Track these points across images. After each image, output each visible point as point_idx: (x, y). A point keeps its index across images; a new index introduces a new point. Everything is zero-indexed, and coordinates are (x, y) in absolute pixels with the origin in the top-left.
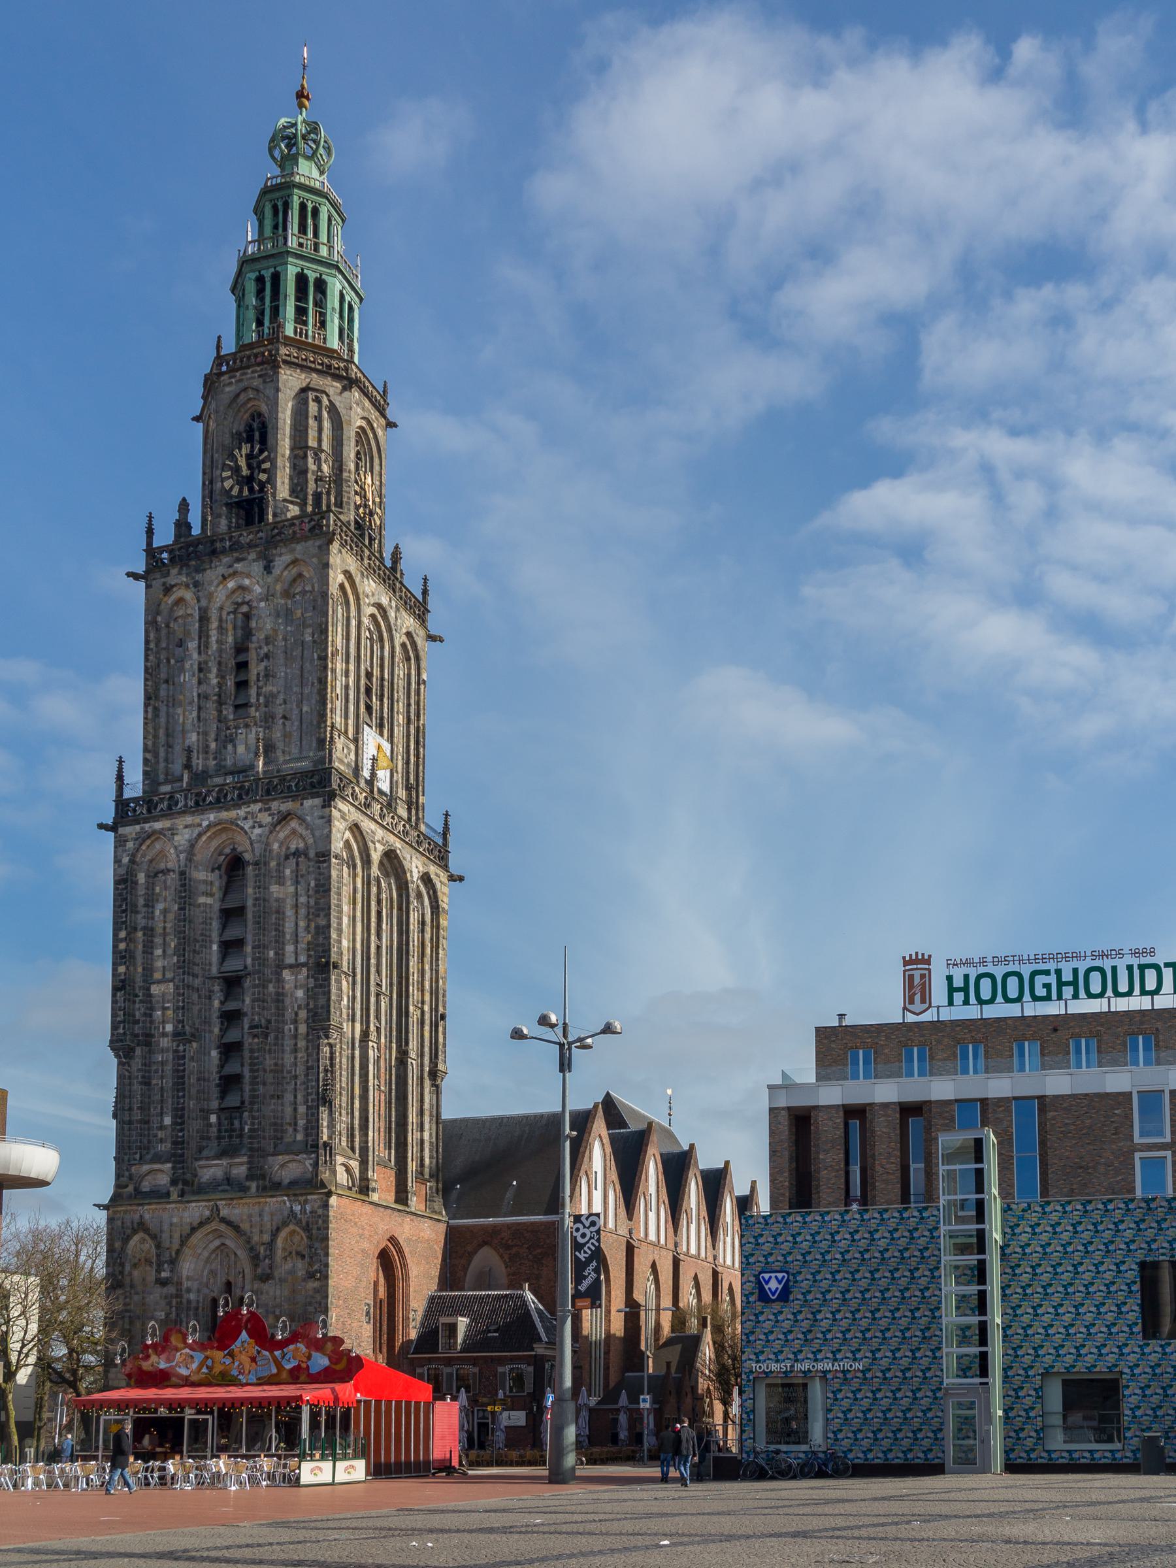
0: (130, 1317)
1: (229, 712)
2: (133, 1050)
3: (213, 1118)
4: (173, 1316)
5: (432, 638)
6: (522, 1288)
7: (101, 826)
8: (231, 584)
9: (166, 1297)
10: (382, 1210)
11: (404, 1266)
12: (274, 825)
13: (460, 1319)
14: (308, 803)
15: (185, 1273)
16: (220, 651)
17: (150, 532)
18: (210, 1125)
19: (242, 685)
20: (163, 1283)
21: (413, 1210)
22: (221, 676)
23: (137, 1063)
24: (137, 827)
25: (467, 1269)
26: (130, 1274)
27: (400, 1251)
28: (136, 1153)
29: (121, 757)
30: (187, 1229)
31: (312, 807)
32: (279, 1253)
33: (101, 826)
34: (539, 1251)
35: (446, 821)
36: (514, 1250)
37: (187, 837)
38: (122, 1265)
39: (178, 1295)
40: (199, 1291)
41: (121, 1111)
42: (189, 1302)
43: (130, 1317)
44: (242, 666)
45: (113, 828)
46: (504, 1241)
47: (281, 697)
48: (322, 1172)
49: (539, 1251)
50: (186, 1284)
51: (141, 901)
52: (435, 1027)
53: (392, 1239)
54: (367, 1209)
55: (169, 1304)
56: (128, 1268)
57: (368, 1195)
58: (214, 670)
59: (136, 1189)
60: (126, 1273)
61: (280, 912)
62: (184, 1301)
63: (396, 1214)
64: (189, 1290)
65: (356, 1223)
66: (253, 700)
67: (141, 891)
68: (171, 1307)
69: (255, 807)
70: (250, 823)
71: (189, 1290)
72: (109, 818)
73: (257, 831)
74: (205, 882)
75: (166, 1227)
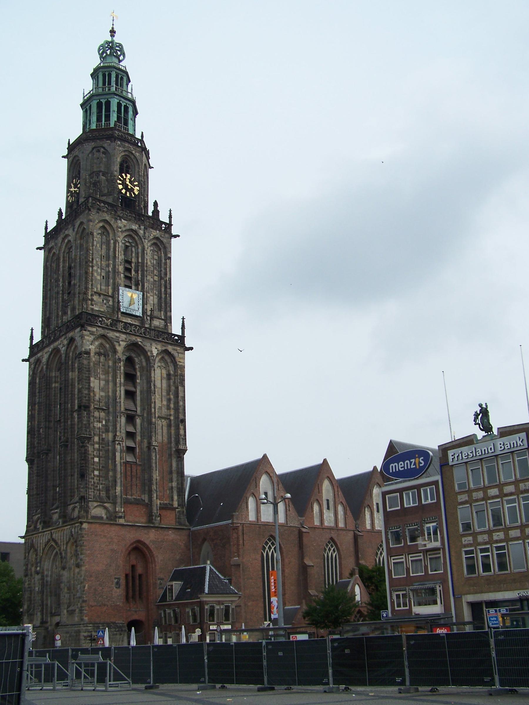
0: (30, 591)
1: (66, 297)
2: (33, 460)
8: (66, 241)
10: (129, 527)
11: (152, 556)
12: (68, 344)
13: (174, 582)
15: (45, 567)
16: (63, 271)
18: (56, 493)
19: (70, 283)
20: (37, 573)
21: (157, 525)
22: (64, 282)
23: (35, 468)
25: (200, 554)
26: (31, 569)
27: (148, 547)
29: (32, 328)
32: (69, 555)
33: (23, 360)
40: (51, 576)
41: (29, 492)
42: (47, 582)
43: (30, 591)
47: (78, 284)
50: (46, 573)
51: (37, 391)
52: (177, 429)
53: (139, 541)
54: (114, 528)
57: (116, 521)
58: (61, 280)
61: (73, 385)
62: (45, 582)
63: (141, 528)
64: (47, 576)
65: (105, 536)
70: (61, 346)
71: (47, 576)
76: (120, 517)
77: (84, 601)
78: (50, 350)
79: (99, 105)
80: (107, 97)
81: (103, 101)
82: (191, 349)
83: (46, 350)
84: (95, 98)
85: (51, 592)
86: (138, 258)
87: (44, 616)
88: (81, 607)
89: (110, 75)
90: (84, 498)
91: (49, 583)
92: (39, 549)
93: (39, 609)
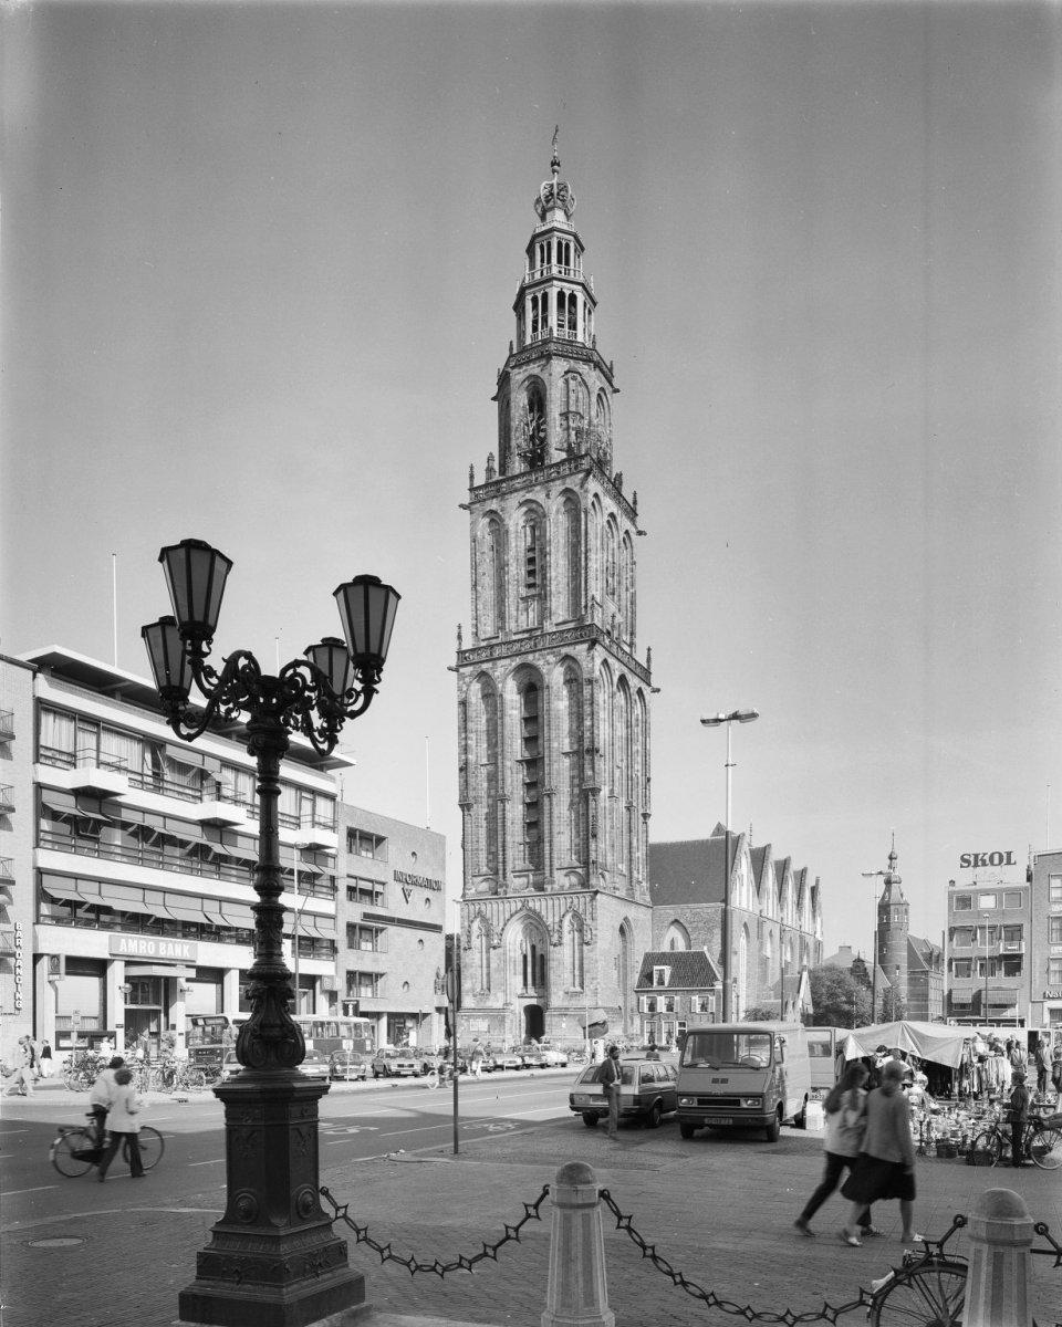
5: (640, 533)
7: (450, 669)
17: (472, 477)
30: (507, 916)
35: (649, 655)
39: (505, 954)
45: (457, 670)
53: (626, 919)
55: (499, 959)
72: (453, 662)
76: (618, 889)
77: (598, 983)
79: (561, 295)
80: (575, 287)
81: (567, 293)
82: (658, 690)
84: (555, 282)
86: (613, 555)
89: (567, 246)
92: (495, 918)
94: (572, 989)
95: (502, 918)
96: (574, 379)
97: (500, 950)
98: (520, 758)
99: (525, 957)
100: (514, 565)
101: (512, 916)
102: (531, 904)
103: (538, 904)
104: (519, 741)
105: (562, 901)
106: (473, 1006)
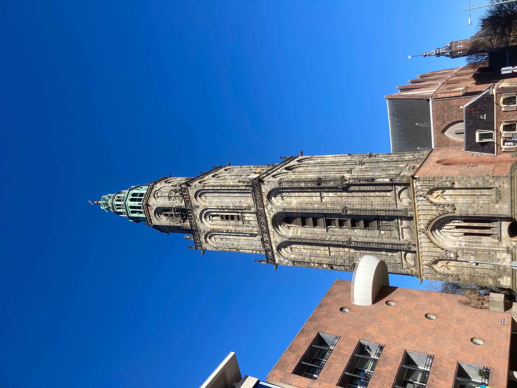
3: (382, 232)
4: (473, 252)
6: (462, 110)
9: (464, 255)
14: (263, 190)
16: (222, 225)
24: (276, 256)
28: (397, 265)
30: (431, 245)
31: (264, 189)
34: (446, 107)
36: (445, 119)
37: (277, 237)
38: (448, 275)
39: (463, 249)
42: (466, 245)
44: (227, 217)
46: (441, 124)
48: (403, 182)
49: (446, 107)
56: (449, 272)
59: (413, 267)
60: (451, 273)
62: (465, 247)
64: (460, 245)
66: (236, 214)
67: (297, 257)
68: (468, 253)
69: (266, 211)
73: (274, 210)
74: (293, 232)
75: (430, 254)
78: (273, 230)
83: (272, 236)
84: (126, 203)
85: (476, 242)
87: (501, 249)
88: (493, 177)
90: (392, 179)
91: (467, 243)
92: (434, 254)
93: (493, 255)
94: (494, 197)
95: (434, 249)
96: (157, 194)
97: (459, 253)
98: (325, 230)
99: (466, 234)
100: (228, 227)
101: (431, 242)
102: (423, 227)
103: (422, 222)
104: (316, 229)
105: (419, 203)
106: (509, 279)
